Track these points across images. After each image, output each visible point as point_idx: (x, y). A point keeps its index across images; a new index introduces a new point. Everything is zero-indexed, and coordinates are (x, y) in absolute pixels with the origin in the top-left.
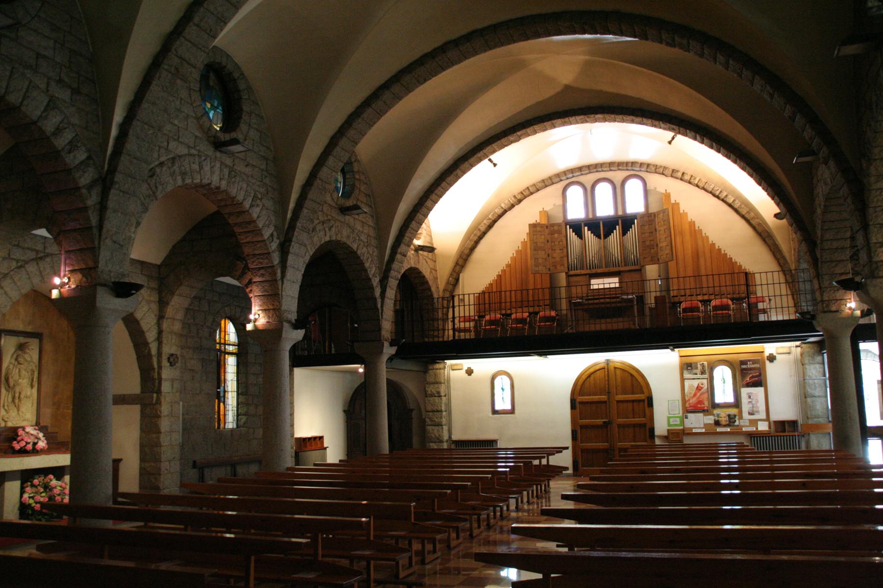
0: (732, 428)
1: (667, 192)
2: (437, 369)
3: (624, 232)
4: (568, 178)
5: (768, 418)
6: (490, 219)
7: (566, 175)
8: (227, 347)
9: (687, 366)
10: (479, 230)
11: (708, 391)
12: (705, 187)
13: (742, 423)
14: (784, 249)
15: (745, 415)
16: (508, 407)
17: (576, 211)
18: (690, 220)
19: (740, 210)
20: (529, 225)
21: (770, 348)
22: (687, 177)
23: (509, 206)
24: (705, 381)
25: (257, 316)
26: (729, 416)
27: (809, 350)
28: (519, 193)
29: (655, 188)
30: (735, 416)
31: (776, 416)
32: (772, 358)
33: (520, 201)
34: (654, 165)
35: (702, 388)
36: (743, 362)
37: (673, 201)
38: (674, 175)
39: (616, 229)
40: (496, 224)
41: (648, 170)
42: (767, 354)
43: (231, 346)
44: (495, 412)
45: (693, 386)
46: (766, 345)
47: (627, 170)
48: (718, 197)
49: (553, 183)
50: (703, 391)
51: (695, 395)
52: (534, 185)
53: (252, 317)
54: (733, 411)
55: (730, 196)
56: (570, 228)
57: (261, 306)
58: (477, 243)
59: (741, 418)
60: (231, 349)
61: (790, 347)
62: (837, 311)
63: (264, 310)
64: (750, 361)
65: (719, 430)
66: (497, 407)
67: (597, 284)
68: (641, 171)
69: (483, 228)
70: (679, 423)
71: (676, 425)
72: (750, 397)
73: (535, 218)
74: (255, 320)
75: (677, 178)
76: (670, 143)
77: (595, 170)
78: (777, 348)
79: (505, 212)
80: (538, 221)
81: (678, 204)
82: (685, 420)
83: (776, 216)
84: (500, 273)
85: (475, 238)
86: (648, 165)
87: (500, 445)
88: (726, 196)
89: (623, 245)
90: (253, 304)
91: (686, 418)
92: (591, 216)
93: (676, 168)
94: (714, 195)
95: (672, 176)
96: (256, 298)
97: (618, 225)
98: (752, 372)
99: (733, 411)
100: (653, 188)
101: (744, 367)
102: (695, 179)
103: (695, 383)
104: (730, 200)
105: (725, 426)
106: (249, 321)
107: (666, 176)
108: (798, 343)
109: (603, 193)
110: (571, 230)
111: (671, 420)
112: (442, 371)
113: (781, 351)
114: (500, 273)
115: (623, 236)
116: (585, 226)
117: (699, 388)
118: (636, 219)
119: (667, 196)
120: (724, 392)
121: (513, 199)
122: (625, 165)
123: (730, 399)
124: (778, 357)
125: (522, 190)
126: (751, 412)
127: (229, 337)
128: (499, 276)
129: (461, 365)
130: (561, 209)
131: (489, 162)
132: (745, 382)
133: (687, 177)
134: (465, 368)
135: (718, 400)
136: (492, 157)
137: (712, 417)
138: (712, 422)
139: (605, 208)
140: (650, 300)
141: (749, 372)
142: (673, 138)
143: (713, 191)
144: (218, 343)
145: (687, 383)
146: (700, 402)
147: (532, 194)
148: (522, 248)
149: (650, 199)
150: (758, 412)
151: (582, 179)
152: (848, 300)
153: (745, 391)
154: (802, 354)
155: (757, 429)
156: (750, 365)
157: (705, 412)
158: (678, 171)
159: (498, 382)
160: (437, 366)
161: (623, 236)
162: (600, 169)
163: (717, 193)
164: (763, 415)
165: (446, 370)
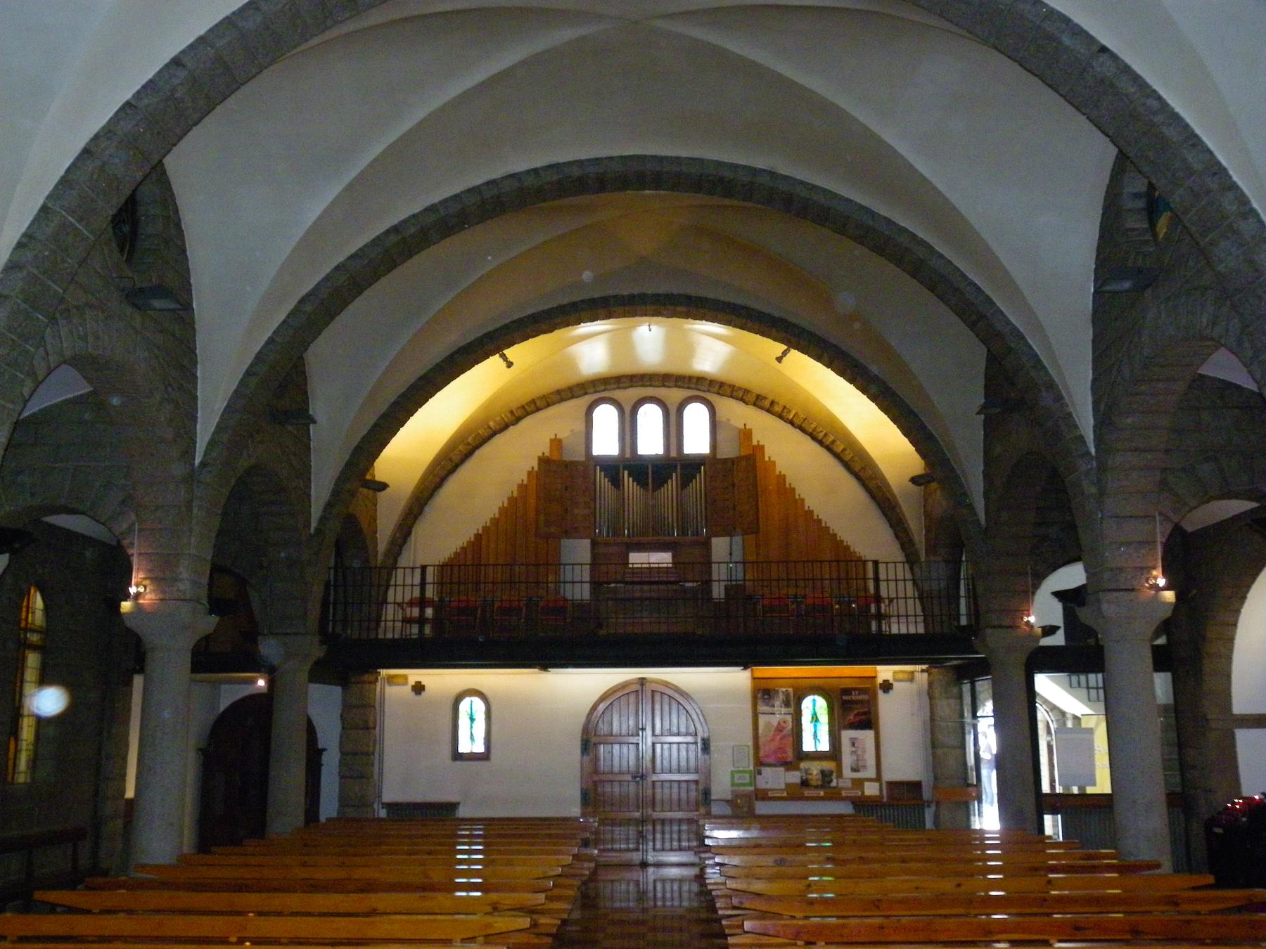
0: (828, 791)
2: (364, 682)
3: (686, 482)
4: (596, 392)
5: (878, 778)
6: (468, 444)
7: (594, 386)
8: (28, 635)
9: (763, 693)
10: (450, 460)
11: (793, 733)
12: (803, 425)
13: (841, 785)
14: (912, 527)
15: (847, 772)
16: (479, 748)
17: (606, 442)
18: (777, 473)
19: (851, 464)
21: (885, 672)
22: (777, 409)
24: (789, 718)
25: (141, 589)
26: (823, 772)
27: (941, 677)
28: (518, 408)
29: (728, 420)
30: (831, 772)
31: (888, 776)
32: (887, 686)
33: (518, 420)
34: (730, 386)
35: (784, 728)
36: (846, 691)
37: (755, 443)
38: (759, 403)
39: (672, 479)
40: (477, 453)
41: (720, 392)
42: (880, 681)
43: (35, 635)
44: (457, 756)
45: (769, 723)
46: (879, 668)
47: (689, 388)
48: (821, 443)
49: (573, 397)
50: (785, 732)
51: (772, 740)
53: (133, 590)
54: (828, 765)
55: (838, 442)
56: (600, 471)
57: (150, 571)
58: (443, 480)
59: (840, 775)
60: (34, 638)
61: (912, 673)
62: (1011, 627)
63: (154, 580)
64: (855, 689)
65: (807, 793)
66: (464, 747)
67: (637, 559)
68: (708, 391)
69: (456, 458)
70: (747, 781)
71: (744, 785)
72: (853, 744)
73: (544, 448)
74: (138, 595)
75: (761, 408)
76: (779, 359)
77: (640, 383)
78: (895, 672)
79: (494, 434)
80: (547, 454)
81: (763, 447)
82: (758, 777)
83: (915, 480)
84: (480, 532)
85: (444, 473)
86: (722, 384)
87: (462, 812)
88: (833, 442)
89: (681, 503)
90: (135, 567)
91: (760, 773)
92: (628, 455)
93: (763, 392)
94: (814, 438)
95: (755, 404)
96: (141, 557)
98: (859, 706)
99: (828, 765)
100: (724, 419)
101: (845, 698)
102: (789, 411)
103: (775, 720)
104: (839, 448)
105: (817, 787)
106: (127, 596)
107: (746, 403)
108: (924, 667)
109: (650, 420)
110: (603, 473)
111: (736, 776)
112: (372, 686)
113: (901, 676)
114: (480, 532)
116: (625, 468)
117: (780, 728)
118: (703, 464)
119: (746, 434)
120: (816, 737)
121: (509, 415)
122: (686, 381)
123: (824, 746)
124: (896, 685)
125: (524, 403)
126: (854, 767)
127: (33, 617)
128: (478, 536)
129: (405, 677)
130: (583, 440)
131: (501, 360)
132: (846, 722)
133: (777, 409)
134: (412, 681)
135: (808, 745)
136: (506, 352)
137: (797, 774)
138: (798, 781)
139: (651, 442)
140: (718, 591)
141: (854, 706)
142: (785, 353)
143: (814, 433)
144: (23, 629)
145: (762, 720)
146: (781, 749)
147: (538, 409)
149: (721, 436)
150: (865, 767)
151: (618, 394)
152: (1026, 612)
153: (847, 735)
154: (930, 684)
155: (863, 793)
156: (855, 696)
157: (789, 766)
158: (765, 398)
159: (464, 706)
160: (367, 677)
161: (682, 489)
162: (648, 383)
163: (820, 436)
164: (871, 773)
165: (379, 685)
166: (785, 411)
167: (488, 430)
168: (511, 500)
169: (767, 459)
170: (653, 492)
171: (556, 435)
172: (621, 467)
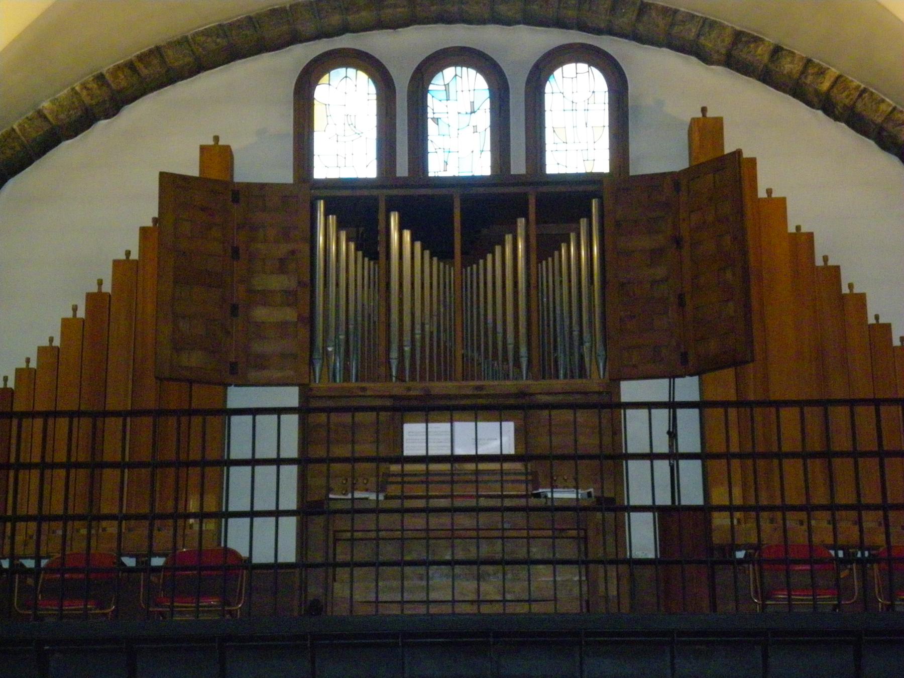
1: (710, 114)
12: (859, 106)
18: (792, 229)
20: (162, 175)
23: (75, 114)
28: (119, 68)
38: (743, 54)
52: (183, 42)
97: (525, 215)
102: (822, 72)
107: (705, 58)
110: (332, 219)
115: (539, 261)
118: (594, 195)
125: (132, 55)
143: (889, 126)
148: (114, 286)
158: (757, 40)
161: (539, 261)
166: (811, 71)
167: (38, 122)
168: (95, 300)
169: (762, 194)
170: (464, 266)
171: (216, 138)
172: (382, 207)
